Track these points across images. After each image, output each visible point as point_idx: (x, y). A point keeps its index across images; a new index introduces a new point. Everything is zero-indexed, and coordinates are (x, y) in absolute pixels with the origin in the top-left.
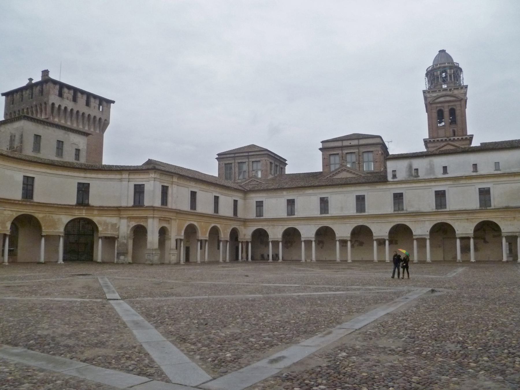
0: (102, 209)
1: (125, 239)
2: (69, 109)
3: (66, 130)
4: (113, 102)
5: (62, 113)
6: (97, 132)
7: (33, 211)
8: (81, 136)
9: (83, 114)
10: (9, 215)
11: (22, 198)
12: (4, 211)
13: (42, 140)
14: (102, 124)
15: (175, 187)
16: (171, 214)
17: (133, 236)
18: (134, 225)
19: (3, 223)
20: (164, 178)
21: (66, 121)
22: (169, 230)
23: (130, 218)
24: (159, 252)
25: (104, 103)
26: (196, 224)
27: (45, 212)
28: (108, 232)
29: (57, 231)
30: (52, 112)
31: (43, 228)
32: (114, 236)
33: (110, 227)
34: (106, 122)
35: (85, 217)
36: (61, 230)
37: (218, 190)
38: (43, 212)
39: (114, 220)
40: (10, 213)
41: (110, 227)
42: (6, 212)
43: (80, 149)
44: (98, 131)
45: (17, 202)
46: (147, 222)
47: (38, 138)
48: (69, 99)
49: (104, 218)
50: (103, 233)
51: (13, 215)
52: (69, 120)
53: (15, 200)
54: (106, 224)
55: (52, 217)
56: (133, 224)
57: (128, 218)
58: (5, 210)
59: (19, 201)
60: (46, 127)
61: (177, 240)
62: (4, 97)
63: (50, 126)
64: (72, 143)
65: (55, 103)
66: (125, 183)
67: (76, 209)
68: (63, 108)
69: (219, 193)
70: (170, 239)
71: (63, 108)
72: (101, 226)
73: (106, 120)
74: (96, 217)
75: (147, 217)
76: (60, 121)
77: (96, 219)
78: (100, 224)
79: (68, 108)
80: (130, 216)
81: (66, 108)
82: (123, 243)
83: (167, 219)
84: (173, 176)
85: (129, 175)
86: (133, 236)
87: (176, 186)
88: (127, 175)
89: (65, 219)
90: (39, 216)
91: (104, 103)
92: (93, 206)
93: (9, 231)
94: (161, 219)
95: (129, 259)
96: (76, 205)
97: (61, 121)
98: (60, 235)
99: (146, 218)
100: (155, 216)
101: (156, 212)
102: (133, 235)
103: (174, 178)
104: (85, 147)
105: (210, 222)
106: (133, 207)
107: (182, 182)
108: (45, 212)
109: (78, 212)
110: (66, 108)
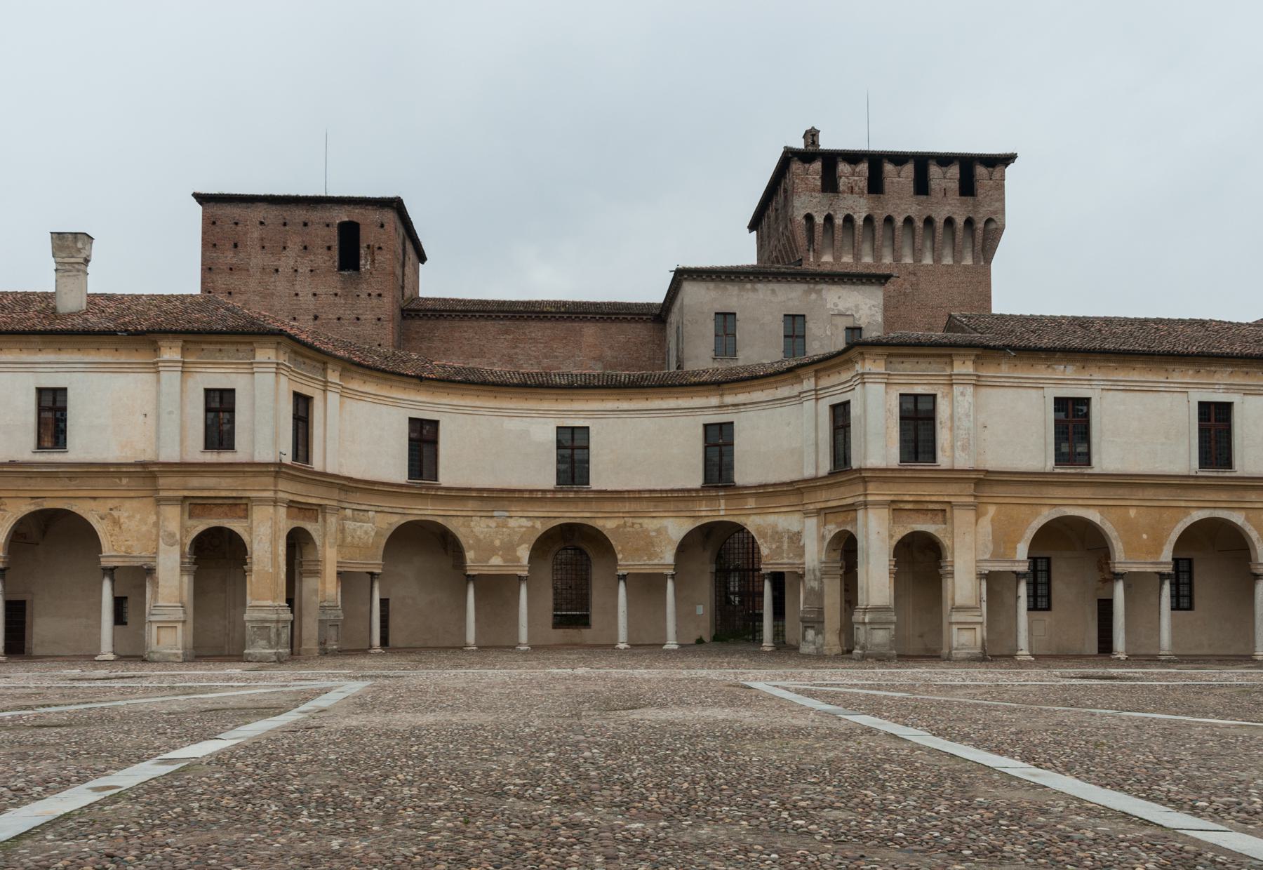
0: (770, 493)
1: (815, 580)
2: (859, 220)
3: (807, 282)
4: (1008, 159)
5: (839, 234)
6: (964, 263)
7: (588, 515)
8: (860, 287)
9: (909, 221)
10: (524, 529)
11: (557, 484)
12: (509, 520)
13: (738, 323)
14: (979, 233)
15: (962, 394)
16: (953, 488)
17: (841, 568)
18: (832, 534)
19: (509, 548)
20: (908, 366)
21: (857, 257)
22: (946, 542)
23: (824, 513)
24: (894, 618)
25: (980, 171)
26: (1094, 516)
27: (621, 515)
28: (783, 558)
29: (656, 561)
30: (811, 240)
31: (620, 556)
32: (797, 570)
33: (785, 546)
34: (992, 226)
35: (726, 519)
36: (669, 557)
37: (1223, 376)
38: (617, 515)
39: (787, 522)
40: (524, 522)
41: (785, 546)
42: (512, 523)
43: (863, 326)
44: (968, 261)
45: (539, 495)
46: (855, 520)
47: (726, 321)
48: (856, 189)
49: (771, 519)
50: (771, 562)
51: (533, 527)
52: (866, 248)
53: (531, 491)
54: (777, 535)
55: (641, 527)
56: (832, 529)
57: (818, 512)
58: (511, 517)
59: (553, 491)
60: (749, 286)
61: (991, 579)
62: (755, 232)
63: (760, 281)
64: (836, 312)
65: (814, 214)
66: (809, 405)
67: (701, 499)
68: (839, 221)
69: (1229, 388)
70: (952, 573)
71: (839, 221)
72: (766, 542)
73: (989, 221)
74: (753, 518)
75: (853, 504)
76: (837, 258)
77: (752, 523)
78: (764, 536)
79: (855, 217)
80: (823, 505)
81: (849, 219)
82: (812, 589)
83: (931, 506)
84: (950, 356)
85: (817, 378)
86: (841, 568)
87: (970, 390)
88: (813, 380)
89: (676, 528)
90: (607, 525)
91: (980, 171)
92: (746, 488)
93: (527, 568)
94: (896, 508)
95: (831, 640)
96: (703, 488)
97: (840, 258)
98: (666, 572)
99: (852, 508)
100: (870, 498)
101: (872, 488)
102: (840, 565)
103: (956, 363)
104: (879, 318)
105: (1183, 504)
106: (831, 474)
107: (1004, 370)
108: (621, 515)
109: (706, 506)
110: (849, 219)
